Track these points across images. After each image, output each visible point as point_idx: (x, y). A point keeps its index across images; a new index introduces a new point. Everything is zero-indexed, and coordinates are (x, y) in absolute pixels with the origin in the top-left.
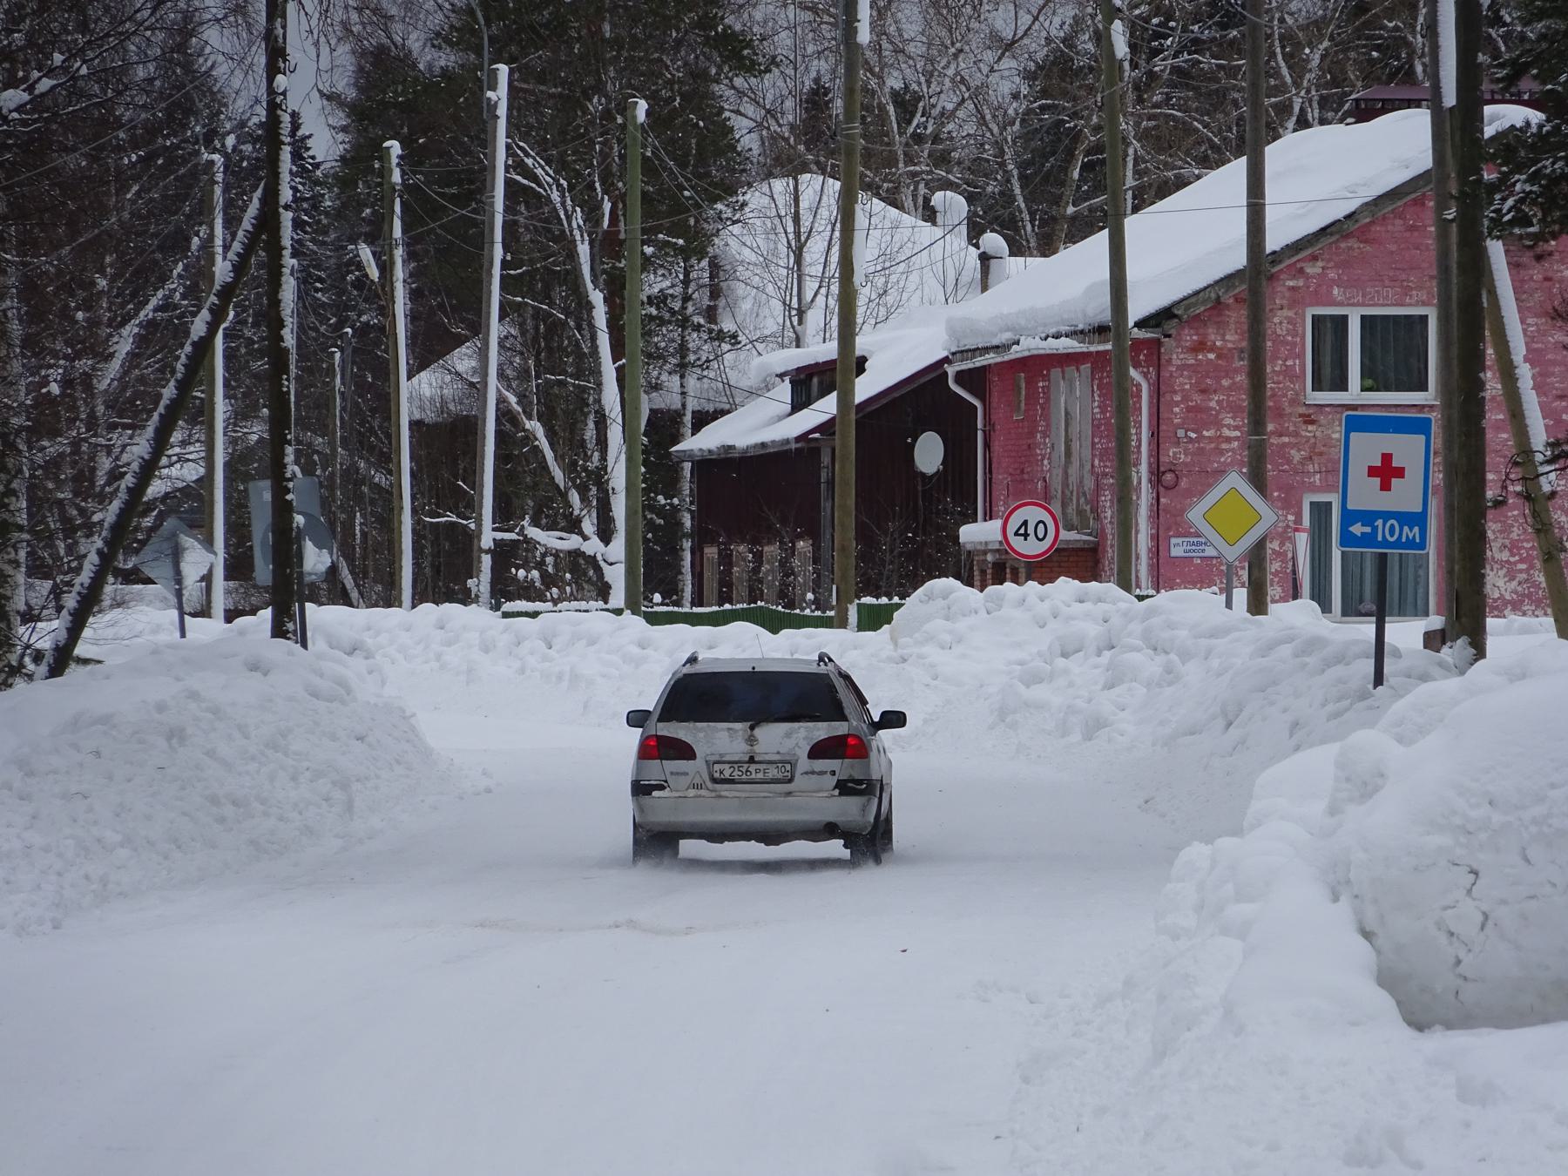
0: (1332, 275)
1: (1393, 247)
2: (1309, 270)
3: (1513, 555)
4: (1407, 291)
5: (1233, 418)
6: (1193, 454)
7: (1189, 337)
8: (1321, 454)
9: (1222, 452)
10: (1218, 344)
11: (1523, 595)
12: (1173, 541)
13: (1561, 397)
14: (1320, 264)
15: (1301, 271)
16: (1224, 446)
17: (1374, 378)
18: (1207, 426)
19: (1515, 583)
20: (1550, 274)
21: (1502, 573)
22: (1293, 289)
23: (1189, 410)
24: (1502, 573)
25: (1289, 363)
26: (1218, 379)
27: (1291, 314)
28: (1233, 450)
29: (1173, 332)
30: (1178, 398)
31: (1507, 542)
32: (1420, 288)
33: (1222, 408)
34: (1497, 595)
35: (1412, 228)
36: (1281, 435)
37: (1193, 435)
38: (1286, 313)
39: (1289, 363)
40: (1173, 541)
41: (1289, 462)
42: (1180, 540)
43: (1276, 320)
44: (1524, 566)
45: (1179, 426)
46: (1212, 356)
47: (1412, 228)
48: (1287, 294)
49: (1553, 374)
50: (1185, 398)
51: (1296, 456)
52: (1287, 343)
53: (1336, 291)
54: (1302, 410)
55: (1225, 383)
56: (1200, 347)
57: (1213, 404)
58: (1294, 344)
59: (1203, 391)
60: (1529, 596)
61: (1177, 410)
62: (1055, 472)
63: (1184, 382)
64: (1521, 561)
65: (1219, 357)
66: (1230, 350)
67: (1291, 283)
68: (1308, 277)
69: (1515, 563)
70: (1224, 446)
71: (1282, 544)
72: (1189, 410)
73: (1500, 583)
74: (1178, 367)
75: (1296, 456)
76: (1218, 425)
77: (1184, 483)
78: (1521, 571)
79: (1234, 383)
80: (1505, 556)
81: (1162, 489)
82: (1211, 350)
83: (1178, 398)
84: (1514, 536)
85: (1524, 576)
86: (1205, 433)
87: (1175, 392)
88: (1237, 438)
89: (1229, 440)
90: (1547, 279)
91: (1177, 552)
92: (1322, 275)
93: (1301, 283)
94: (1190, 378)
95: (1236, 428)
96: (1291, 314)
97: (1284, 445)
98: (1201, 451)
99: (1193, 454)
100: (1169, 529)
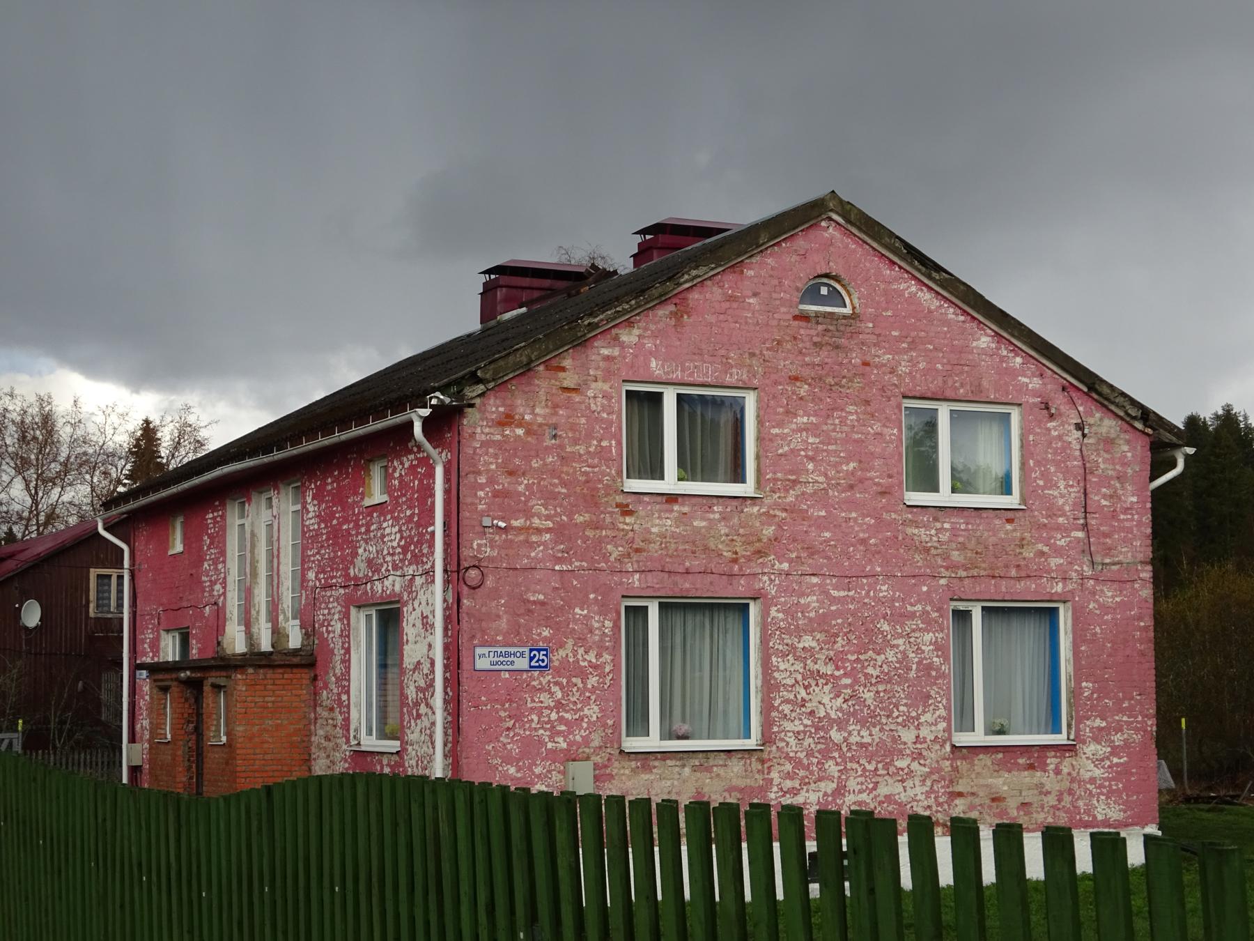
0: (649, 345)
1: (711, 318)
2: (624, 338)
3: (838, 668)
4: (727, 367)
5: (545, 506)
6: (500, 547)
7: (495, 406)
8: (637, 550)
9: (532, 546)
10: (527, 417)
11: (849, 714)
12: (479, 651)
13: (883, 493)
14: (636, 332)
15: (616, 338)
16: (534, 538)
17: (687, 469)
18: (515, 514)
19: (840, 700)
20: (868, 359)
21: (827, 689)
22: (608, 358)
23: (496, 494)
24: (827, 689)
25: (604, 444)
26: (528, 459)
27: (606, 387)
28: (544, 544)
29: (478, 401)
30: (482, 480)
31: (832, 653)
32: (740, 366)
33: (532, 493)
34: (822, 714)
35: (731, 299)
36: (597, 526)
37: (502, 524)
38: (600, 384)
39: (604, 444)
40: (479, 651)
41: (605, 558)
42: (485, 650)
43: (590, 393)
44: (848, 681)
45: (482, 514)
46: (520, 432)
47: (731, 299)
48: (602, 364)
49: (872, 468)
50: (491, 481)
51: (614, 551)
52: (602, 420)
53: (653, 364)
54: (620, 499)
55: (535, 464)
56: (507, 420)
57: (521, 488)
58: (611, 422)
59: (511, 473)
60: (854, 714)
61: (481, 494)
62: (229, 595)
63: (489, 462)
64: (845, 675)
65: (528, 432)
66: (540, 425)
67: (605, 352)
68: (622, 346)
69: (839, 678)
70: (534, 538)
71: (599, 656)
72: (496, 494)
73: (826, 700)
74: (486, 444)
75: (614, 551)
76: (528, 514)
77: (489, 583)
78: (846, 686)
79: (545, 464)
80: (829, 669)
81: (465, 590)
82: (520, 425)
83: (482, 480)
84: (838, 646)
85: (849, 691)
86: (516, 523)
87: (479, 473)
88: (548, 530)
89: (539, 531)
90: (866, 364)
91: (482, 664)
92: (639, 346)
93: (616, 352)
94: (496, 456)
95: (548, 518)
96: (606, 387)
97: (600, 541)
98: (509, 544)
99: (500, 547)
100: (473, 637)
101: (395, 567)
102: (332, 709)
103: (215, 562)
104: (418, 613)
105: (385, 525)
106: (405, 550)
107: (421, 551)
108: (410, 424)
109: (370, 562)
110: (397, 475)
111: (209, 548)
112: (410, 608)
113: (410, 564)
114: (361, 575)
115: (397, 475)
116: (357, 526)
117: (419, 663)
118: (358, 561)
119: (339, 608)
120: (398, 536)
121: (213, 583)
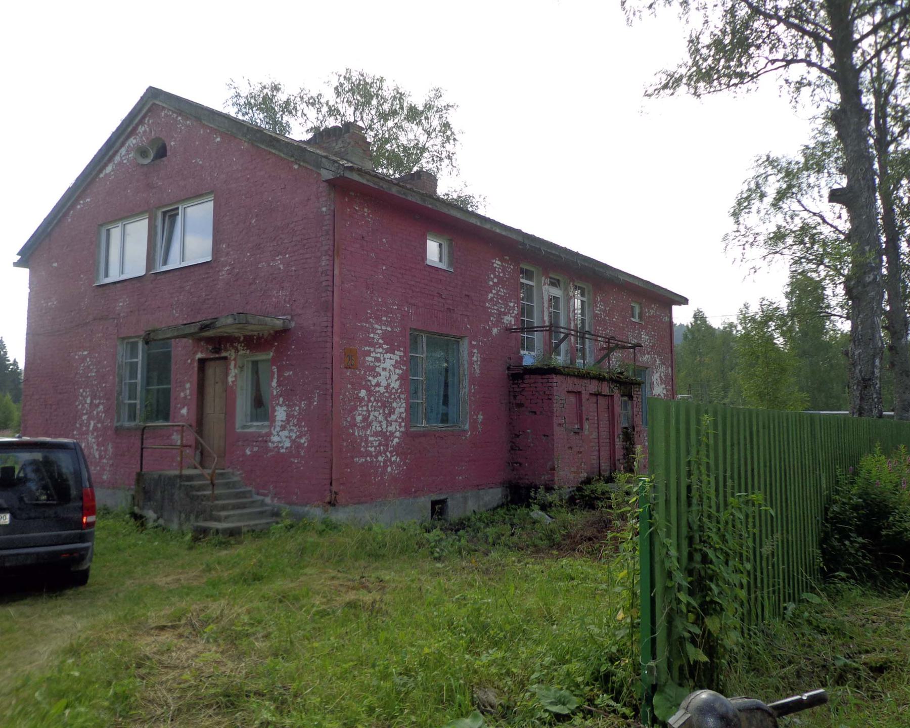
101: (648, 353)
103: (505, 300)
106: (652, 347)
121: (501, 314)
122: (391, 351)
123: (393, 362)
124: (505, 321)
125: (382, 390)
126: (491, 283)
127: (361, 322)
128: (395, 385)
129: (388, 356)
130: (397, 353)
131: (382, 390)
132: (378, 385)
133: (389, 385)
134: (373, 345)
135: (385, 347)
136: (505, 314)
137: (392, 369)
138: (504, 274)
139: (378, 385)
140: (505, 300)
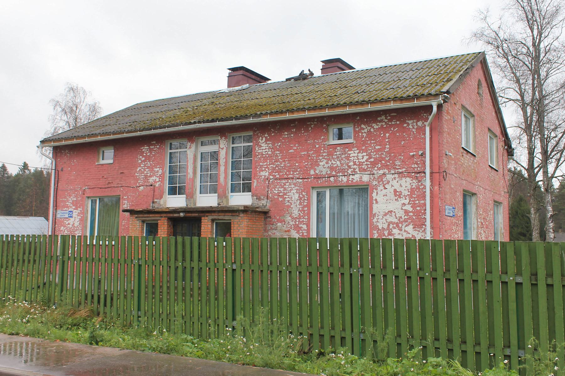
12: (446, 207)
40: (446, 207)
62: (165, 182)
101: (362, 170)
102: (289, 231)
103: (151, 168)
104: (390, 189)
105: (349, 152)
106: (374, 164)
107: (394, 163)
108: (431, 107)
109: (332, 168)
110: (366, 131)
111: (142, 161)
112: (381, 187)
113: (379, 169)
114: (324, 173)
115: (366, 131)
116: (318, 152)
117: (391, 212)
118: (321, 168)
119: (297, 188)
120: (366, 158)
122: (76, 209)
123: (77, 213)
124: (150, 181)
125: (71, 226)
126: (140, 161)
127: (62, 198)
128: (77, 224)
129: (75, 211)
130: (79, 209)
131: (71, 226)
132: (69, 224)
133: (74, 224)
134: (68, 207)
135: (74, 207)
136: (151, 176)
137: (76, 216)
138: (151, 153)
139: (69, 224)
140: (151, 168)
